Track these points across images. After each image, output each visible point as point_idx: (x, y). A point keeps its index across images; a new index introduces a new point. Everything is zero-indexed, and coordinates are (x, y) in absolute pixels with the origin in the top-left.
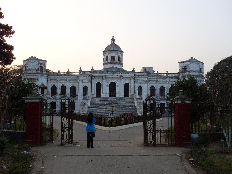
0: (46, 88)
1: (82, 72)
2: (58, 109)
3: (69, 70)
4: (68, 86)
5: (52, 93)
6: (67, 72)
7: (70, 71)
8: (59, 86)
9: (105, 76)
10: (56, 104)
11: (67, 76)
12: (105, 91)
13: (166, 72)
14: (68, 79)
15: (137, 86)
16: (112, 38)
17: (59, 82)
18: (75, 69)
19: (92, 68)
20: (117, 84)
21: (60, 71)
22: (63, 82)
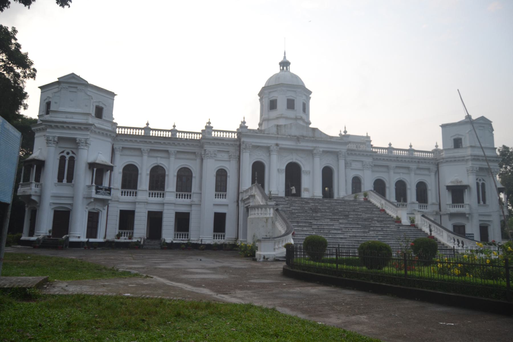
0: (110, 168)
1: (213, 133)
2: (141, 229)
3: (174, 126)
4: (172, 168)
5: (124, 186)
6: (169, 131)
7: (178, 128)
8: (145, 166)
9: (277, 145)
10: (136, 214)
11: (171, 142)
12: (276, 183)
13: (408, 148)
14: (172, 149)
15: (352, 174)
16: (281, 59)
17: (145, 157)
18: (191, 125)
19: (244, 122)
20: (303, 169)
21: (151, 126)
22: (157, 157)
